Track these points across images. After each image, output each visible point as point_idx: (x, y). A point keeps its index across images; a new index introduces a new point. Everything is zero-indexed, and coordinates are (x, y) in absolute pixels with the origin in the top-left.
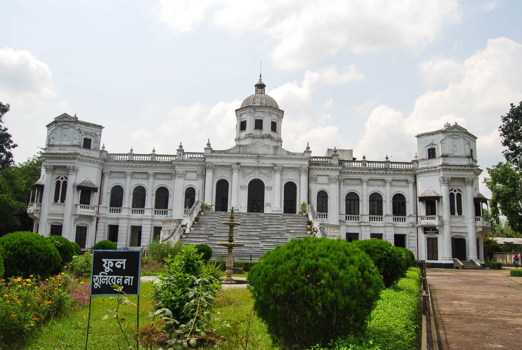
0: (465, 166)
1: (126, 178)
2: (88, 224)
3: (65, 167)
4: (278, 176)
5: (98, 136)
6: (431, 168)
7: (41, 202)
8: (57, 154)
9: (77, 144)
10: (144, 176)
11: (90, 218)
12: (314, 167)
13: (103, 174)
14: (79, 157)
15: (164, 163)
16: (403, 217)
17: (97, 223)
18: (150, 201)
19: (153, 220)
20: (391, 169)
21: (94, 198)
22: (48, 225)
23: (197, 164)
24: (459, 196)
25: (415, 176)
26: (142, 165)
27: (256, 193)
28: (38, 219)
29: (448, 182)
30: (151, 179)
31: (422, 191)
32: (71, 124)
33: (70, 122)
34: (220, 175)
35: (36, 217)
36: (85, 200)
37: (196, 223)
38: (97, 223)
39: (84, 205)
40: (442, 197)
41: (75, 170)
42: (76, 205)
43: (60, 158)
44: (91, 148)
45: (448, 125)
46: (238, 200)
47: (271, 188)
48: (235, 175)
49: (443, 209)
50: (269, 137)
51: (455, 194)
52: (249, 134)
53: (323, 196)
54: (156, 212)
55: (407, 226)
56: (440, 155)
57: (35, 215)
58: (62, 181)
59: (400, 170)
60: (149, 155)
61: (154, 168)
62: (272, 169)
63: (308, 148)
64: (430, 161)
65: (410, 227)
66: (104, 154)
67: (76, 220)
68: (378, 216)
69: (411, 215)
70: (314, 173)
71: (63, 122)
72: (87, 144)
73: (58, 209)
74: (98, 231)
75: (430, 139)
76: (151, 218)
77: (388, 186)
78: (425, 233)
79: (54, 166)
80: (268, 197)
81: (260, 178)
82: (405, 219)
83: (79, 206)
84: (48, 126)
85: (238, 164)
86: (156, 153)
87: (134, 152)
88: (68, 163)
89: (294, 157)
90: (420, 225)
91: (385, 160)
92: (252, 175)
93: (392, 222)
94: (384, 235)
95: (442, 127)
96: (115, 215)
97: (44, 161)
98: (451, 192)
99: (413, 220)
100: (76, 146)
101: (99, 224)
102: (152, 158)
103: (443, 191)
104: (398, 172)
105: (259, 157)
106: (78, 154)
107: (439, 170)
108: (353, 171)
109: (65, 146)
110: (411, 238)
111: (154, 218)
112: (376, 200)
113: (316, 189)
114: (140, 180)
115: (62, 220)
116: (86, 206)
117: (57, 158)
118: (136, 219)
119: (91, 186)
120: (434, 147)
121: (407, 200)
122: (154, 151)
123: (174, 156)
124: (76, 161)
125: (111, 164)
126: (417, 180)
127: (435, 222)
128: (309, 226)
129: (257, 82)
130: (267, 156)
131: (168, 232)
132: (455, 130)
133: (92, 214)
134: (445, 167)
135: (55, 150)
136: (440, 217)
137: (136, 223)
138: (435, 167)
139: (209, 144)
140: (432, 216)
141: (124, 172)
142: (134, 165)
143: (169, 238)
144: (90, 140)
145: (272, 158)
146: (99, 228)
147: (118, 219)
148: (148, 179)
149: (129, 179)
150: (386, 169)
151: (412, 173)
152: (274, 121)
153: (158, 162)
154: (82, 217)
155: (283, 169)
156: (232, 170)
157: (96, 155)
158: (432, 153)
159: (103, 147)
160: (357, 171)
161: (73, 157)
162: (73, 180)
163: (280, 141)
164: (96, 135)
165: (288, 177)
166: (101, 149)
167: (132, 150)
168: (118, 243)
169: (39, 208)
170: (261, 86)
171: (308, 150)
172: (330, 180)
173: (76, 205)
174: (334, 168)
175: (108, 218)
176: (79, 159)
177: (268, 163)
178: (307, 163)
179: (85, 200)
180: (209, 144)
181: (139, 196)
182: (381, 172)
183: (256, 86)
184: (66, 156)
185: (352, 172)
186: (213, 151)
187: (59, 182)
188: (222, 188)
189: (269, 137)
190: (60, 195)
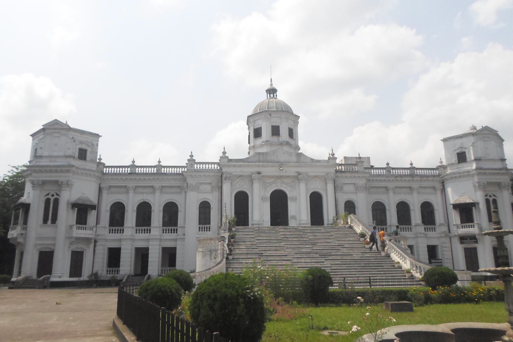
0: (500, 169)
1: (128, 193)
2: (85, 247)
3: (56, 182)
4: (303, 186)
5: (95, 146)
6: (464, 172)
7: (25, 222)
8: (47, 166)
9: (71, 154)
10: (150, 190)
11: (87, 240)
12: (339, 175)
13: (100, 190)
14: (74, 169)
15: (171, 174)
16: (433, 226)
17: (95, 246)
18: (157, 217)
19: (161, 240)
20: (417, 175)
21: (92, 216)
23: (211, 174)
24: (495, 201)
25: (443, 183)
26: (147, 178)
27: (279, 203)
28: (23, 245)
29: (483, 186)
30: (158, 193)
31: (453, 198)
32: (62, 132)
33: (62, 129)
34: (238, 186)
35: (19, 243)
36: (82, 220)
37: (232, 240)
38: (95, 246)
39: (80, 226)
40: (478, 203)
41: (68, 184)
42: (71, 227)
43: (51, 171)
44: (87, 159)
45: (474, 128)
46: (260, 212)
47: (295, 199)
48: (256, 186)
49: (481, 216)
50: (288, 143)
51: (491, 199)
52: (267, 141)
53: (350, 207)
54: (163, 230)
55: (439, 236)
56: (473, 158)
57: (20, 240)
58: (52, 199)
59: (427, 176)
60: (154, 167)
61: (161, 180)
62: (298, 178)
63: (333, 155)
64: (460, 165)
65: (442, 237)
66: (101, 166)
67: (71, 243)
68: (407, 226)
69: (441, 225)
71: (55, 129)
72: (83, 154)
73: (48, 230)
74: (96, 256)
75: (459, 142)
76: (159, 237)
77: (415, 194)
78: (462, 243)
79: (43, 181)
80: (292, 209)
82: (434, 229)
83: (75, 227)
84: (33, 135)
85: (259, 173)
86: (162, 164)
87: (136, 164)
88: (61, 177)
89: (318, 164)
90: (456, 234)
91: (409, 166)
92: (274, 185)
93: (423, 231)
94: (415, 247)
95: (467, 130)
96: (117, 236)
97: (30, 175)
98: (486, 197)
99: (445, 229)
100: (70, 156)
101: (97, 248)
102: (157, 170)
103: (479, 197)
104: (425, 178)
105: (281, 164)
106: (73, 166)
107: (473, 174)
108: (379, 179)
109: (56, 157)
110: (445, 249)
111: (162, 238)
112: (403, 209)
113: (343, 199)
114: (145, 195)
116: (83, 226)
117: (46, 172)
118: (141, 239)
119: (88, 203)
120: (464, 150)
121: (436, 207)
122: (159, 162)
123: (182, 167)
124: (70, 174)
125: (110, 177)
126: (446, 186)
127: (474, 230)
128: (362, 239)
129: (268, 87)
130: (290, 164)
131: (209, 253)
132: (486, 132)
133: (90, 236)
134: (480, 171)
135: (44, 162)
136: (478, 224)
137: (142, 245)
138: (468, 172)
139: (224, 153)
140: (472, 224)
141: (126, 187)
142: (138, 178)
143: (222, 260)
144: (85, 151)
145: (295, 166)
146: (97, 252)
147: (120, 240)
148: (154, 192)
149: (131, 194)
150: (412, 176)
151: (438, 178)
152: (291, 127)
153: (165, 174)
154: (79, 240)
155: (308, 179)
156: (252, 181)
157: (94, 167)
158: (462, 157)
159: (100, 159)
160: (383, 179)
161: (68, 169)
162: (67, 197)
163: (298, 148)
164: (93, 144)
166: (98, 161)
167: (133, 162)
168: (121, 268)
169: (23, 232)
170: (272, 91)
171: (332, 157)
172: (357, 189)
173: (71, 227)
174: (361, 175)
175: (106, 240)
177: (291, 171)
178: (333, 170)
179: (82, 220)
180: (224, 153)
181: (144, 213)
182: (408, 179)
183: (267, 91)
184: (59, 169)
185: (377, 180)
186: (231, 160)
188: (242, 201)
189: (288, 143)
190: (51, 213)
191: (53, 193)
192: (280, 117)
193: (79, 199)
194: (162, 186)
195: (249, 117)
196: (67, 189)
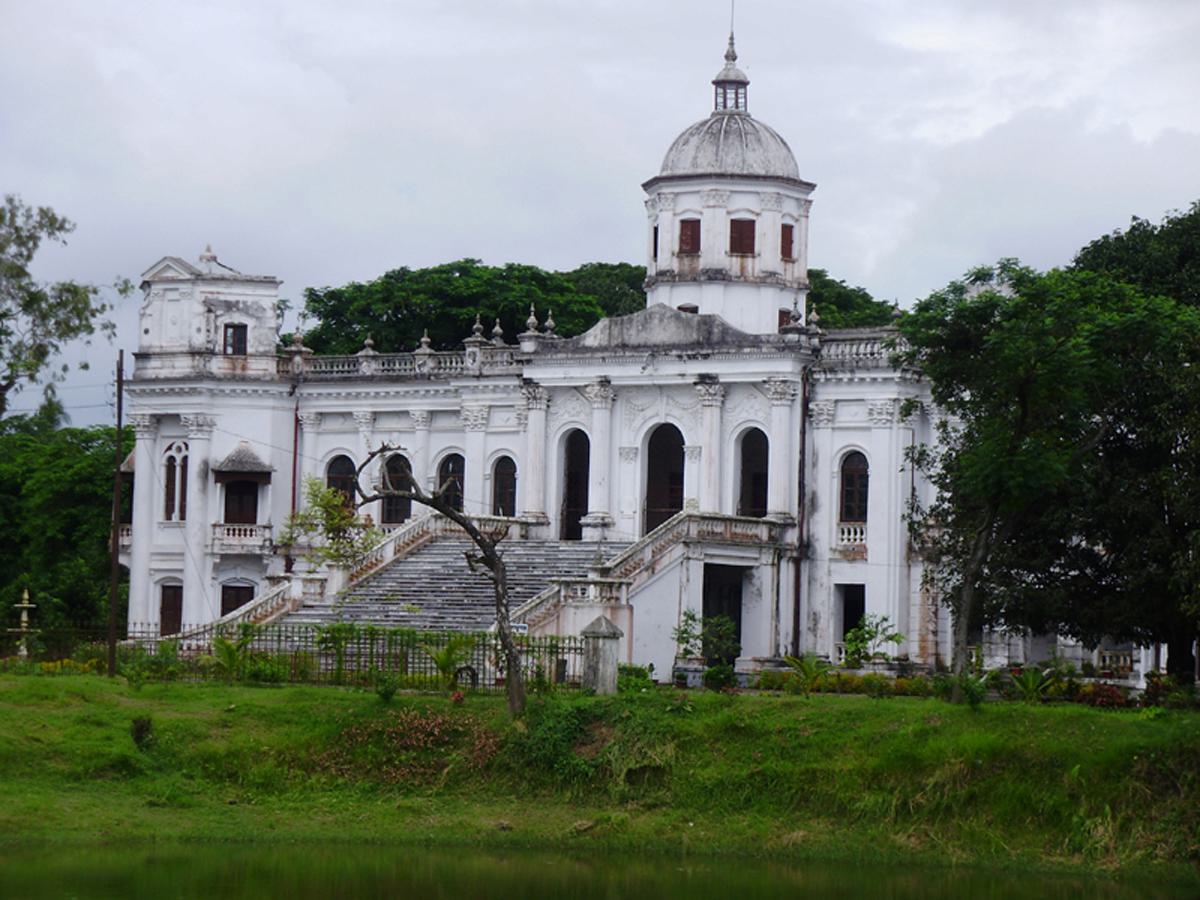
13: (297, 421)
22: (152, 585)
32: (184, 288)
34: (566, 416)
41: (205, 425)
67: (216, 568)
70: (825, 394)
81: (671, 420)
85: (605, 382)
92: (649, 413)
113: (829, 447)
115: (181, 571)
119: (247, 468)
129: (718, 68)
165: (744, 416)
176: (211, 390)
187: (171, 459)
191: (179, 443)
192: (698, 192)
193: (230, 460)
194: (432, 413)
195: (646, 186)
196: (200, 435)
